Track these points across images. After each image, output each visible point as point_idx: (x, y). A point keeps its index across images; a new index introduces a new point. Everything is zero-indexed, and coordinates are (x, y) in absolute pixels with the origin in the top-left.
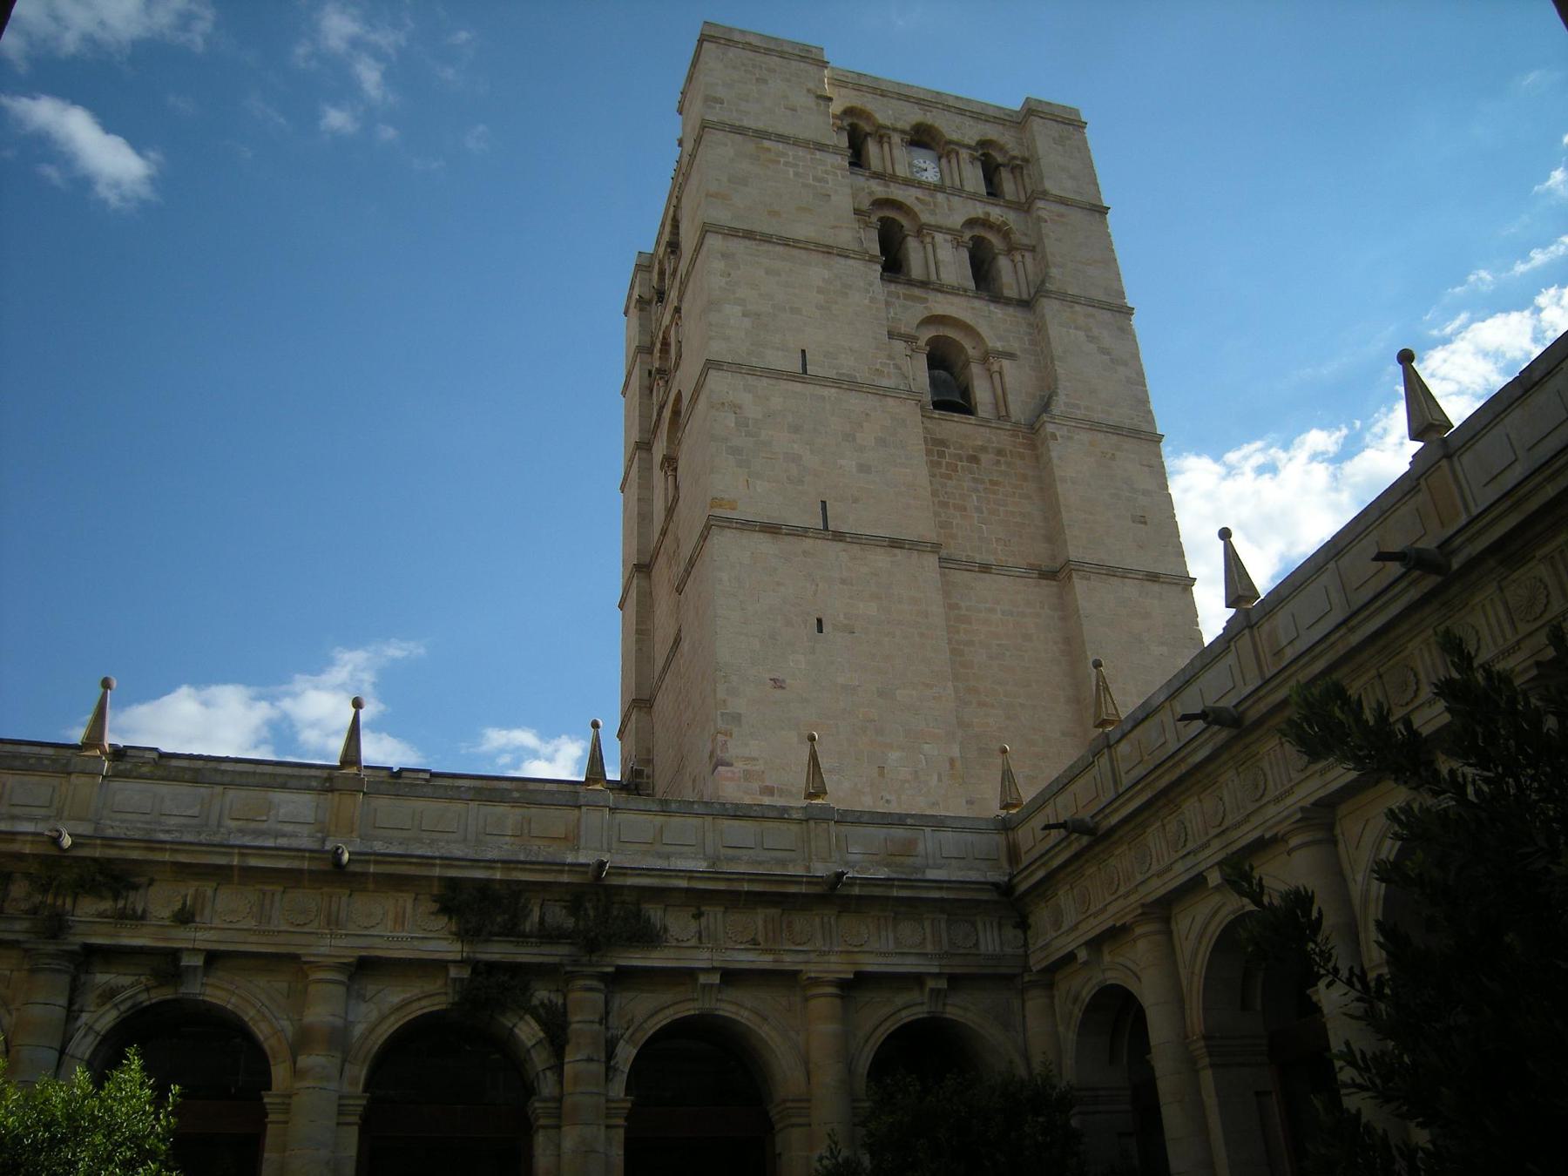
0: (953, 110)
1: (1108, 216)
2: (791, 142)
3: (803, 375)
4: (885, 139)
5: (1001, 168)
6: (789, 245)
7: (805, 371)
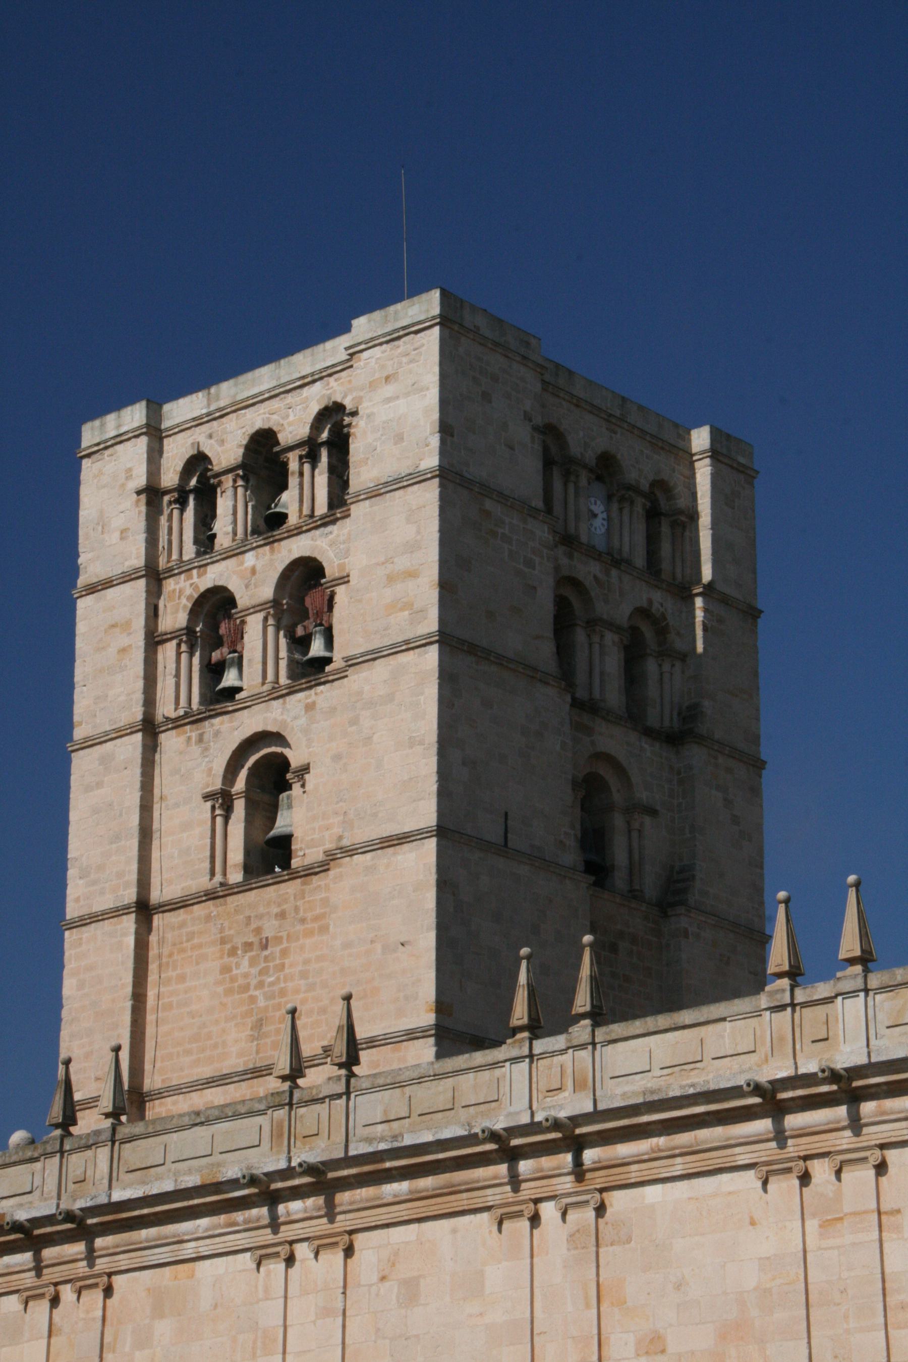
0: (636, 431)
1: (759, 620)
2: (509, 504)
3: (504, 848)
4: (572, 478)
5: (663, 518)
6: (502, 664)
7: (506, 845)
